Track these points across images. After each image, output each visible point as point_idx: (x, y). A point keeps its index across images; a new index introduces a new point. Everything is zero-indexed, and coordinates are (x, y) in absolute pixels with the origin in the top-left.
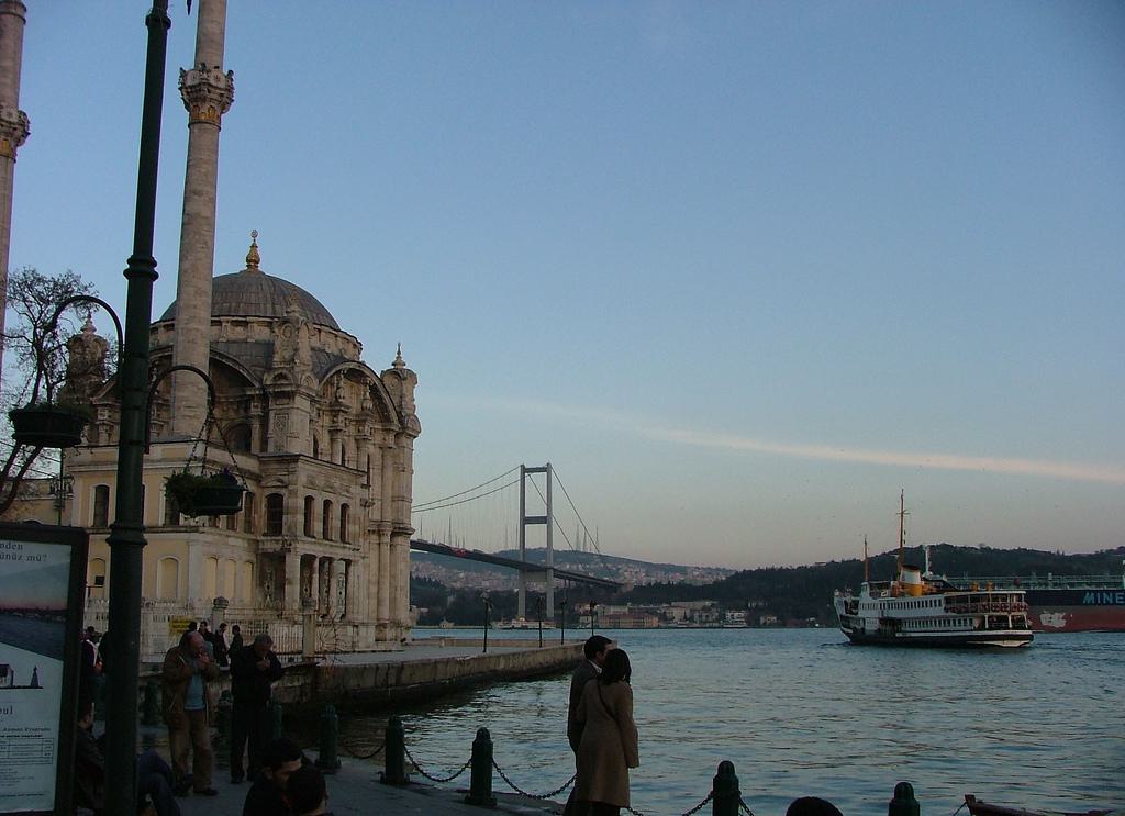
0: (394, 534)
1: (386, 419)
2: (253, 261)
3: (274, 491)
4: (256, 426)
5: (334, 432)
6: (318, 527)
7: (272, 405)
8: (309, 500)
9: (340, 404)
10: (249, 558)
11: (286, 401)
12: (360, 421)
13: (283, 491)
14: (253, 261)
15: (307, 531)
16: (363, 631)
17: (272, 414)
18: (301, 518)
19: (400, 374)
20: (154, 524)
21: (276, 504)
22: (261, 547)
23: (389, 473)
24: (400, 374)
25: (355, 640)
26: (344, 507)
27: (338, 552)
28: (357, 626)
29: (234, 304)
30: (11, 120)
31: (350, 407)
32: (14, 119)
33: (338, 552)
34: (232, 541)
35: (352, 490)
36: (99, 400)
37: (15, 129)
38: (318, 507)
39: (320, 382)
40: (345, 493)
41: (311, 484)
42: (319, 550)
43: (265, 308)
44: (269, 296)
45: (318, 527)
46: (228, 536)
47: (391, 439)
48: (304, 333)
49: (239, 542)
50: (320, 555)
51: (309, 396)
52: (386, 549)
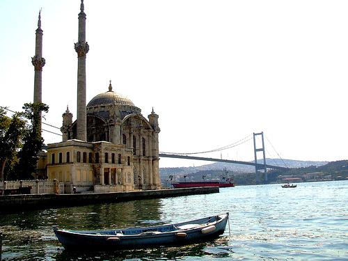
2: (110, 89)
5: (130, 134)
6: (110, 160)
8: (106, 154)
14: (110, 89)
15: (107, 161)
18: (103, 159)
19: (153, 116)
21: (97, 154)
24: (153, 116)
33: (118, 167)
38: (110, 155)
42: (111, 166)
45: (110, 160)
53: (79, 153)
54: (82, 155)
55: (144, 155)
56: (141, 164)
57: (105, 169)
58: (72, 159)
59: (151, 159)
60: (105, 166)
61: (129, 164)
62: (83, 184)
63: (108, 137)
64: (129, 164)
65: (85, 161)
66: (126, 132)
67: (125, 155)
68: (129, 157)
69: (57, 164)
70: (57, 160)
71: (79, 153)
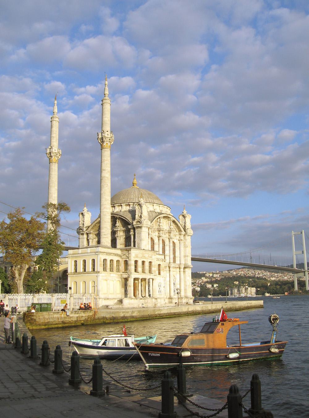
0: (185, 268)
1: (180, 231)
3: (125, 259)
4: (132, 237)
5: (159, 237)
7: (136, 231)
8: (136, 262)
9: (160, 228)
10: (118, 280)
11: (140, 229)
12: (170, 232)
13: (127, 259)
15: (136, 271)
16: (159, 300)
17: (136, 233)
18: (132, 268)
20: (88, 271)
21: (126, 263)
22: (122, 276)
23: (182, 248)
25: (156, 303)
26: (150, 262)
27: (147, 276)
28: (156, 299)
29: (126, 199)
30: (56, 152)
31: (164, 229)
32: (56, 151)
34: (112, 275)
35: (153, 257)
36: (88, 231)
37: (57, 154)
39: (151, 222)
40: (151, 258)
41: (137, 256)
42: (140, 276)
43: (136, 200)
44: (137, 195)
45: (140, 269)
46: (110, 274)
47: (182, 236)
48: (144, 207)
49: (115, 275)
50: (141, 278)
51: (147, 227)
52: (182, 273)
53: (105, 260)
54: (108, 263)
55: (174, 261)
56: (171, 272)
57: (135, 279)
58: (99, 267)
59: (182, 267)
60: (134, 275)
61: (159, 274)
62: (110, 296)
63: (134, 242)
64: (159, 274)
65: (111, 270)
66: (155, 235)
67: (155, 263)
68: (159, 265)
69: (80, 273)
70: (80, 268)
71: (105, 260)
